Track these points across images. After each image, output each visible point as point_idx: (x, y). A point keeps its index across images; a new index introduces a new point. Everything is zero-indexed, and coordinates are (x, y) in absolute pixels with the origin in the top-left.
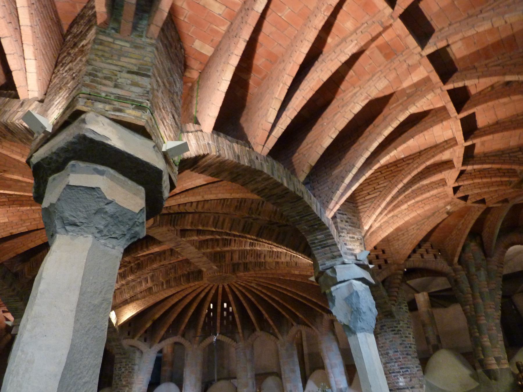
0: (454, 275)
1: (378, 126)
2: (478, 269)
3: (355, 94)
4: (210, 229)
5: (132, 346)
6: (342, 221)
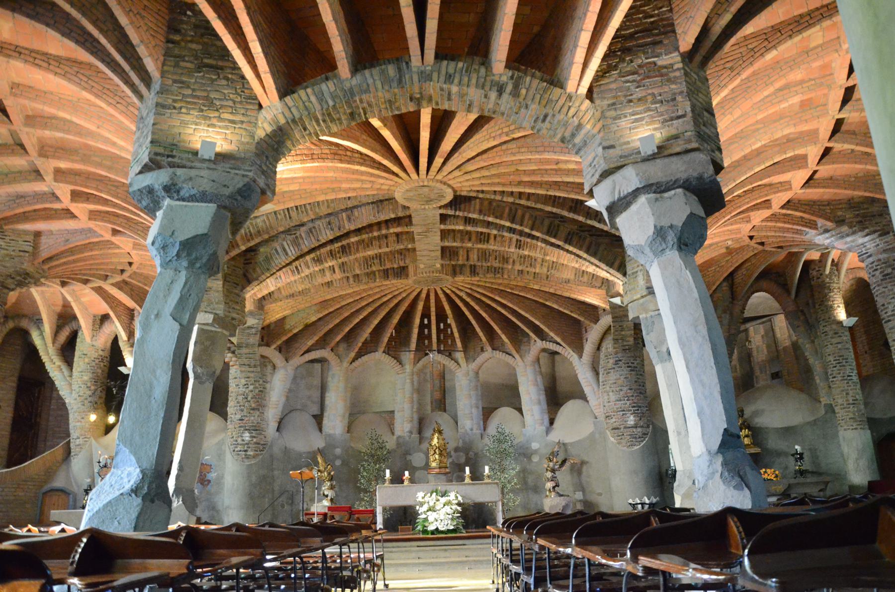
4: (503, 222)
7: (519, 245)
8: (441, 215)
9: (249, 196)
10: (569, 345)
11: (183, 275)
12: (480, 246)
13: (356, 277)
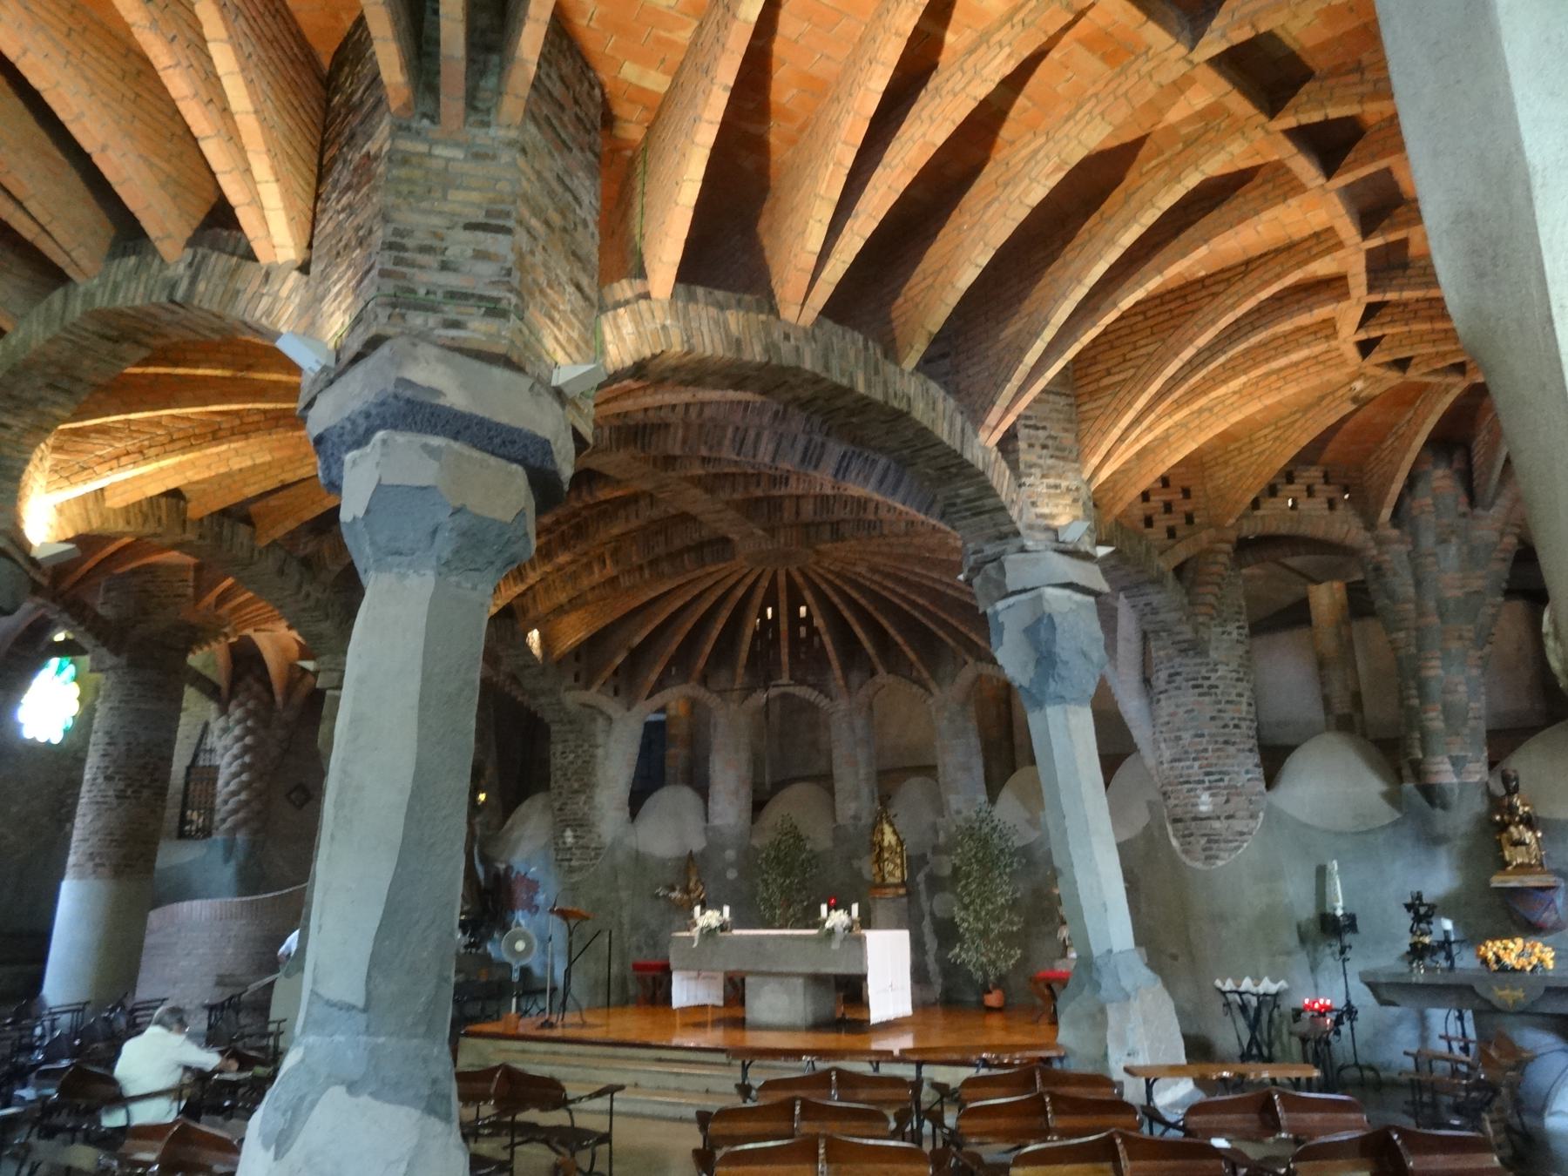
0: (1374, 552)
1: (1109, 219)
2: (1442, 541)
3: (1036, 152)
5: (584, 705)
6: (1031, 446)
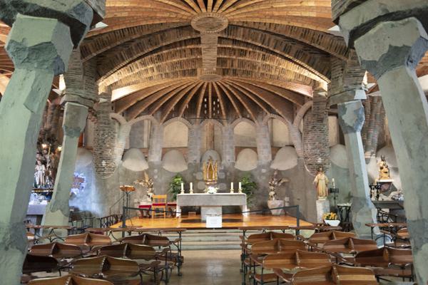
4: (257, 44)
7: (264, 59)
8: (219, 37)
9: (83, 13)
10: (287, 116)
11: (33, 75)
12: (240, 58)
13: (167, 75)
